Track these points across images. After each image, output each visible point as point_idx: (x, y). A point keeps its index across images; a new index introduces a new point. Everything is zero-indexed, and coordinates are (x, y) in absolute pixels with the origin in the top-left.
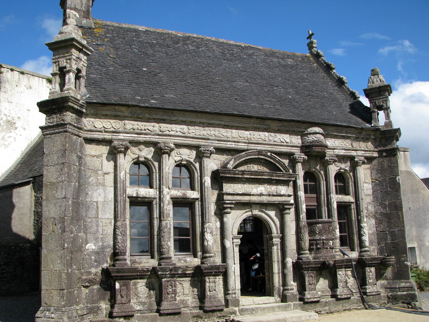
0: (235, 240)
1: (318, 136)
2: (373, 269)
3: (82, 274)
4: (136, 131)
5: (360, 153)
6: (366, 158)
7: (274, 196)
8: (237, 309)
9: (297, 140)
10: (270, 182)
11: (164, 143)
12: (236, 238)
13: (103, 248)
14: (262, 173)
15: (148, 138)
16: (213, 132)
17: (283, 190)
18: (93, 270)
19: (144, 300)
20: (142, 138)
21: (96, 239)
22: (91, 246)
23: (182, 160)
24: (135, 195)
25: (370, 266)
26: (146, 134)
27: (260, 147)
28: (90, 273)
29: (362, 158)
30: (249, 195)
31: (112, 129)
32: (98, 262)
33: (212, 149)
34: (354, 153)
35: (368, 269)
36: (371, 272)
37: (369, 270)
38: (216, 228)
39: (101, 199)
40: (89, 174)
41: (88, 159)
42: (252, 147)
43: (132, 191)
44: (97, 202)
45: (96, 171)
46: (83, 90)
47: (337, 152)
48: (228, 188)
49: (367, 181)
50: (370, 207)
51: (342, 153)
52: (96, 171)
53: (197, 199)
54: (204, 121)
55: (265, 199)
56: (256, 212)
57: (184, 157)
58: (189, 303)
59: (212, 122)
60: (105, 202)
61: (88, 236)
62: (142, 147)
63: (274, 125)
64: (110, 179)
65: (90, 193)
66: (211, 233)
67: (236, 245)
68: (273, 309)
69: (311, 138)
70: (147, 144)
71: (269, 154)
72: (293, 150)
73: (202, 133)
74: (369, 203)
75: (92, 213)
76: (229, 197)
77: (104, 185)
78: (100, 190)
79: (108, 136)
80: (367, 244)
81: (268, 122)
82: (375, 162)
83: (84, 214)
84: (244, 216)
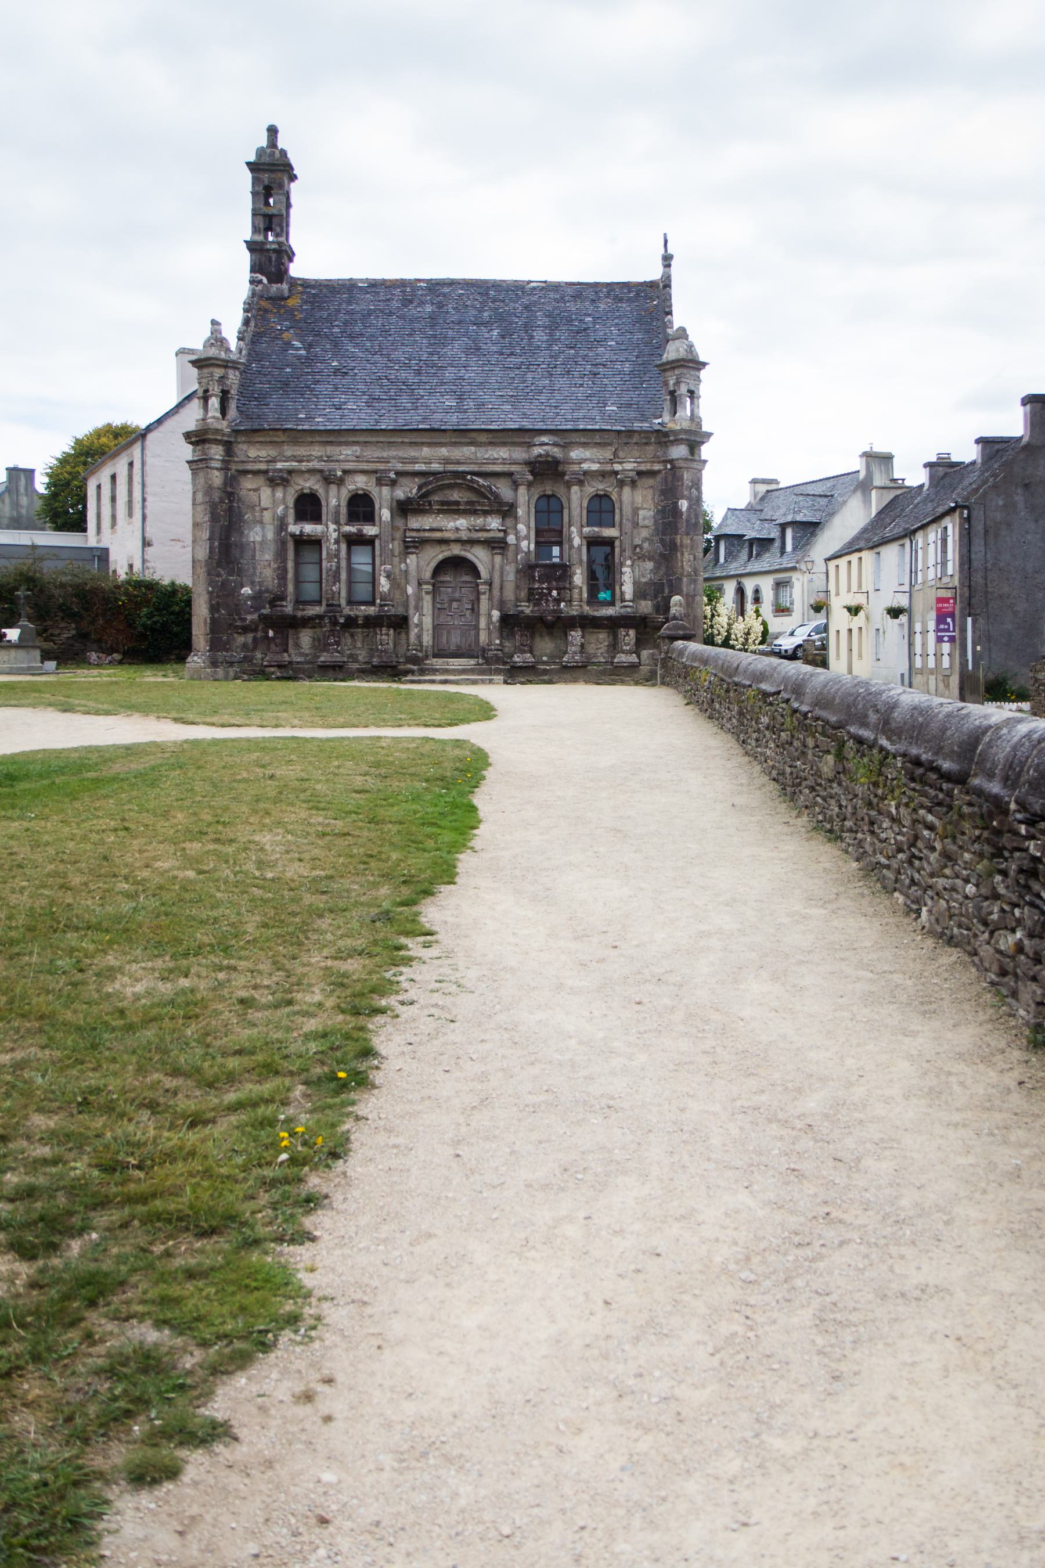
0: (424, 587)
1: (545, 448)
2: (632, 633)
3: (234, 620)
4: (298, 458)
5: (629, 466)
6: (640, 473)
7: (476, 531)
8: (416, 668)
9: (519, 454)
10: (474, 512)
11: (330, 471)
12: (427, 583)
13: (260, 592)
14: (457, 503)
15: (312, 465)
16: (395, 453)
17: (494, 523)
18: (249, 617)
19: (307, 652)
20: (304, 466)
21: (252, 584)
22: (247, 590)
23: (357, 489)
24: (298, 533)
25: (627, 626)
26: (308, 461)
27: (461, 468)
28: (245, 620)
29: (632, 474)
30: (442, 530)
31: (269, 458)
32: (257, 609)
33: (392, 475)
34: (617, 467)
35: (622, 632)
36: (627, 635)
37: (624, 633)
38: (401, 570)
39: (258, 539)
40: (244, 511)
41: (243, 493)
42: (451, 468)
43: (294, 528)
44: (254, 542)
45: (253, 507)
46: (232, 412)
47: (585, 466)
48: (415, 522)
49: (645, 506)
50: (646, 545)
51: (595, 467)
52: (253, 507)
53: (376, 536)
54: (382, 439)
55: (464, 535)
56: (456, 550)
57: (359, 485)
58: (360, 658)
59: (392, 440)
60: (263, 542)
61: (244, 579)
62: (307, 475)
63: (483, 438)
64: (267, 516)
65: (246, 532)
66: (388, 577)
67: (427, 593)
68: (464, 672)
69: (537, 451)
70: (312, 471)
71: (469, 477)
72: (514, 468)
73: (380, 455)
74: (646, 539)
75: (248, 554)
76: (414, 534)
77: (261, 522)
78: (258, 529)
79: (263, 467)
80: (629, 596)
81: (473, 434)
82: (659, 478)
83: (238, 556)
84: (441, 557)
